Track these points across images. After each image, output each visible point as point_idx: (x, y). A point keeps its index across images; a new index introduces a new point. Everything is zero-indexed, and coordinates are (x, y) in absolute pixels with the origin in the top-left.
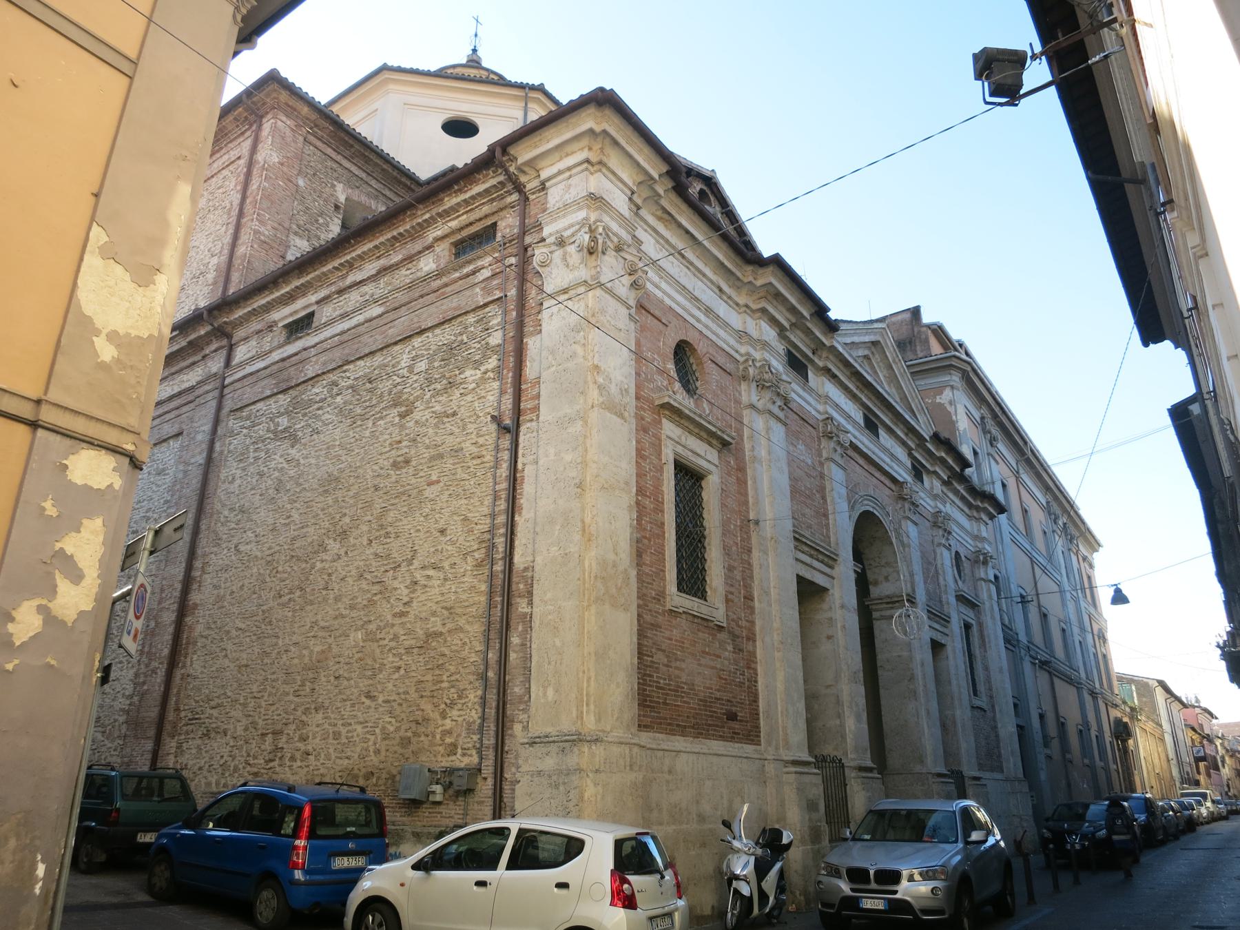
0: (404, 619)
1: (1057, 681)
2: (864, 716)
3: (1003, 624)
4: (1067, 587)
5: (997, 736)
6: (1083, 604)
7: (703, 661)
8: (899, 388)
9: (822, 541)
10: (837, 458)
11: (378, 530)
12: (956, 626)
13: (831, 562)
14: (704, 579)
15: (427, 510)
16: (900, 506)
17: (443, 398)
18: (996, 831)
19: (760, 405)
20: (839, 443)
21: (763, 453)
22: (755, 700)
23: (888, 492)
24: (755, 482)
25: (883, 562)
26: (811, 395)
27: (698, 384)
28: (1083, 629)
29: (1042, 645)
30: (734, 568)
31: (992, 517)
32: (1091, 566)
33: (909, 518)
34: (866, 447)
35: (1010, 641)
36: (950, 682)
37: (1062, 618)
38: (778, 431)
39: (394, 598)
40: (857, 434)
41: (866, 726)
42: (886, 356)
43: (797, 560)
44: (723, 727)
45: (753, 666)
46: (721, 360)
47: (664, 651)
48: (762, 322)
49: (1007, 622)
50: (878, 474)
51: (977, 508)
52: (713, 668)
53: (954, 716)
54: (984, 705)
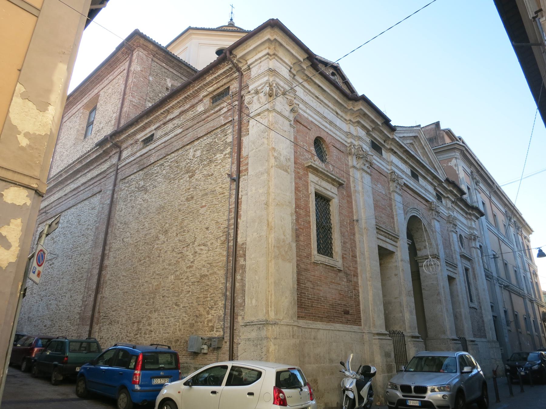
0: (191, 269)
1: (513, 295)
2: (414, 312)
3: (484, 268)
4: (516, 249)
5: (483, 321)
7: (331, 286)
8: (428, 157)
9: (391, 229)
10: (398, 191)
11: (180, 229)
12: (460, 269)
13: (395, 239)
14: (331, 248)
15: (201, 219)
16: (430, 213)
17: (207, 168)
18: (479, 366)
19: (358, 166)
20: (398, 184)
21: (360, 188)
22: (358, 304)
23: (424, 207)
24: (356, 202)
25: (423, 240)
26: (384, 162)
27: (327, 157)
28: (525, 270)
29: (505, 278)
30: (347, 243)
31: (477, 218)
32: (529, 241)
33: (435, 219)
35: (488, 276)
36: (458, 296)
37: (515, 265)
38: (367, 178)
39: (187, 260)
40: (407, 179)
41: (415, 317)
43: (378, 238)
44: (342, 317)
45: (357, 288)
46: (338, 146)
47: (311, 282)
48: (358, 128)
49: (487, 268)
50: (419, 198)
51: (470, 214)
52: (336, 289)
53: (460, 312)
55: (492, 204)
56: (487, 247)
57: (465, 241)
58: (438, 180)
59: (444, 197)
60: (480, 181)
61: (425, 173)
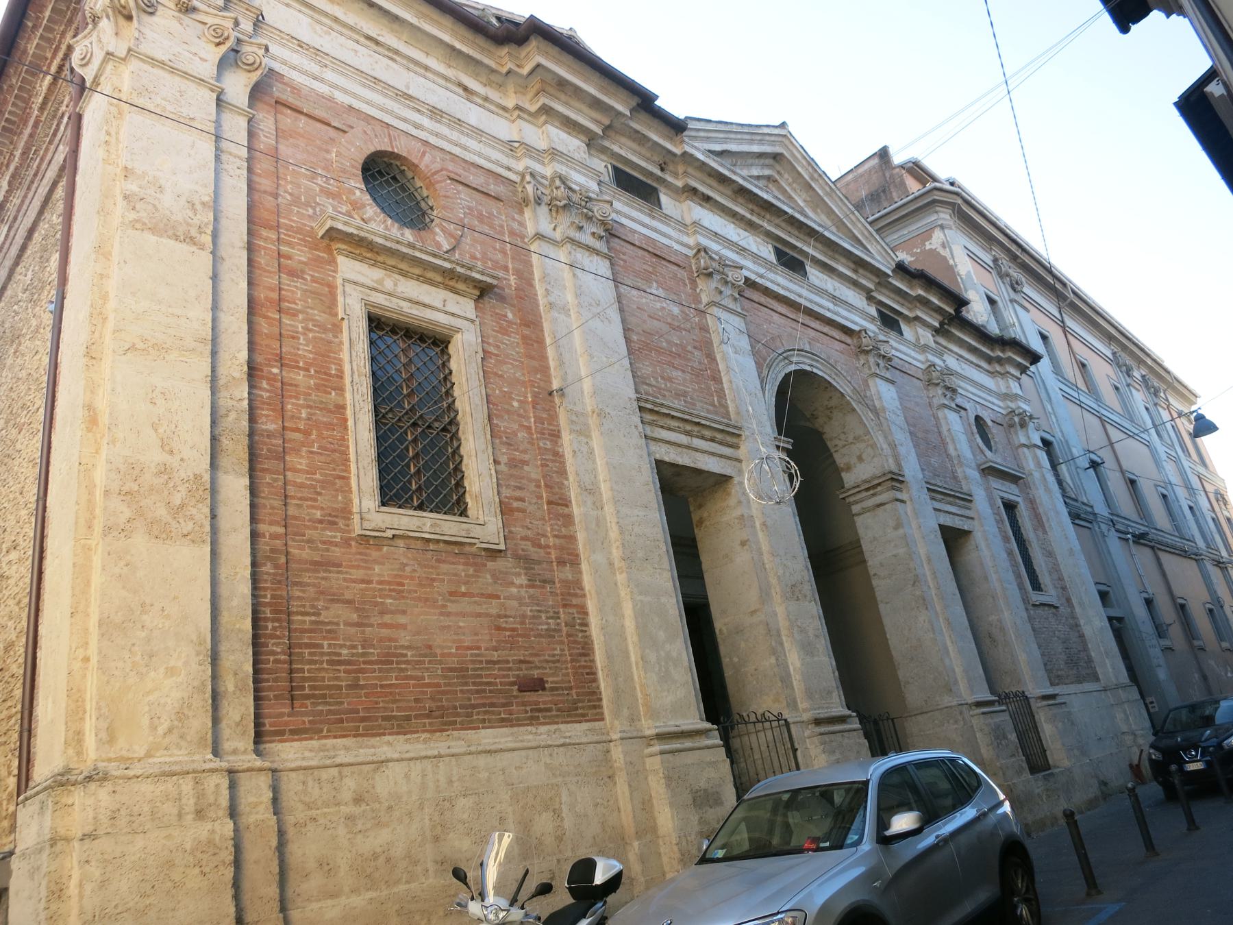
5: (1082, 636)
6: (1186, 464)
7: (452, 607)
8: (830, 212)
16: (862, 362)
22: (586, 650)
26: (669, 225)
29: (1135, 517)
31: (1024, 370)
35: (1080, 516)
36: (986, 578)
42: (799, 174)
47: (349, 602)
51: (999, 361)
52: (479, 615)
53: (1000, 621)
54: (1055, 602)
56: (1067, 441)
58: (871, 272)
59: (908, 320)
61: (826, 255)
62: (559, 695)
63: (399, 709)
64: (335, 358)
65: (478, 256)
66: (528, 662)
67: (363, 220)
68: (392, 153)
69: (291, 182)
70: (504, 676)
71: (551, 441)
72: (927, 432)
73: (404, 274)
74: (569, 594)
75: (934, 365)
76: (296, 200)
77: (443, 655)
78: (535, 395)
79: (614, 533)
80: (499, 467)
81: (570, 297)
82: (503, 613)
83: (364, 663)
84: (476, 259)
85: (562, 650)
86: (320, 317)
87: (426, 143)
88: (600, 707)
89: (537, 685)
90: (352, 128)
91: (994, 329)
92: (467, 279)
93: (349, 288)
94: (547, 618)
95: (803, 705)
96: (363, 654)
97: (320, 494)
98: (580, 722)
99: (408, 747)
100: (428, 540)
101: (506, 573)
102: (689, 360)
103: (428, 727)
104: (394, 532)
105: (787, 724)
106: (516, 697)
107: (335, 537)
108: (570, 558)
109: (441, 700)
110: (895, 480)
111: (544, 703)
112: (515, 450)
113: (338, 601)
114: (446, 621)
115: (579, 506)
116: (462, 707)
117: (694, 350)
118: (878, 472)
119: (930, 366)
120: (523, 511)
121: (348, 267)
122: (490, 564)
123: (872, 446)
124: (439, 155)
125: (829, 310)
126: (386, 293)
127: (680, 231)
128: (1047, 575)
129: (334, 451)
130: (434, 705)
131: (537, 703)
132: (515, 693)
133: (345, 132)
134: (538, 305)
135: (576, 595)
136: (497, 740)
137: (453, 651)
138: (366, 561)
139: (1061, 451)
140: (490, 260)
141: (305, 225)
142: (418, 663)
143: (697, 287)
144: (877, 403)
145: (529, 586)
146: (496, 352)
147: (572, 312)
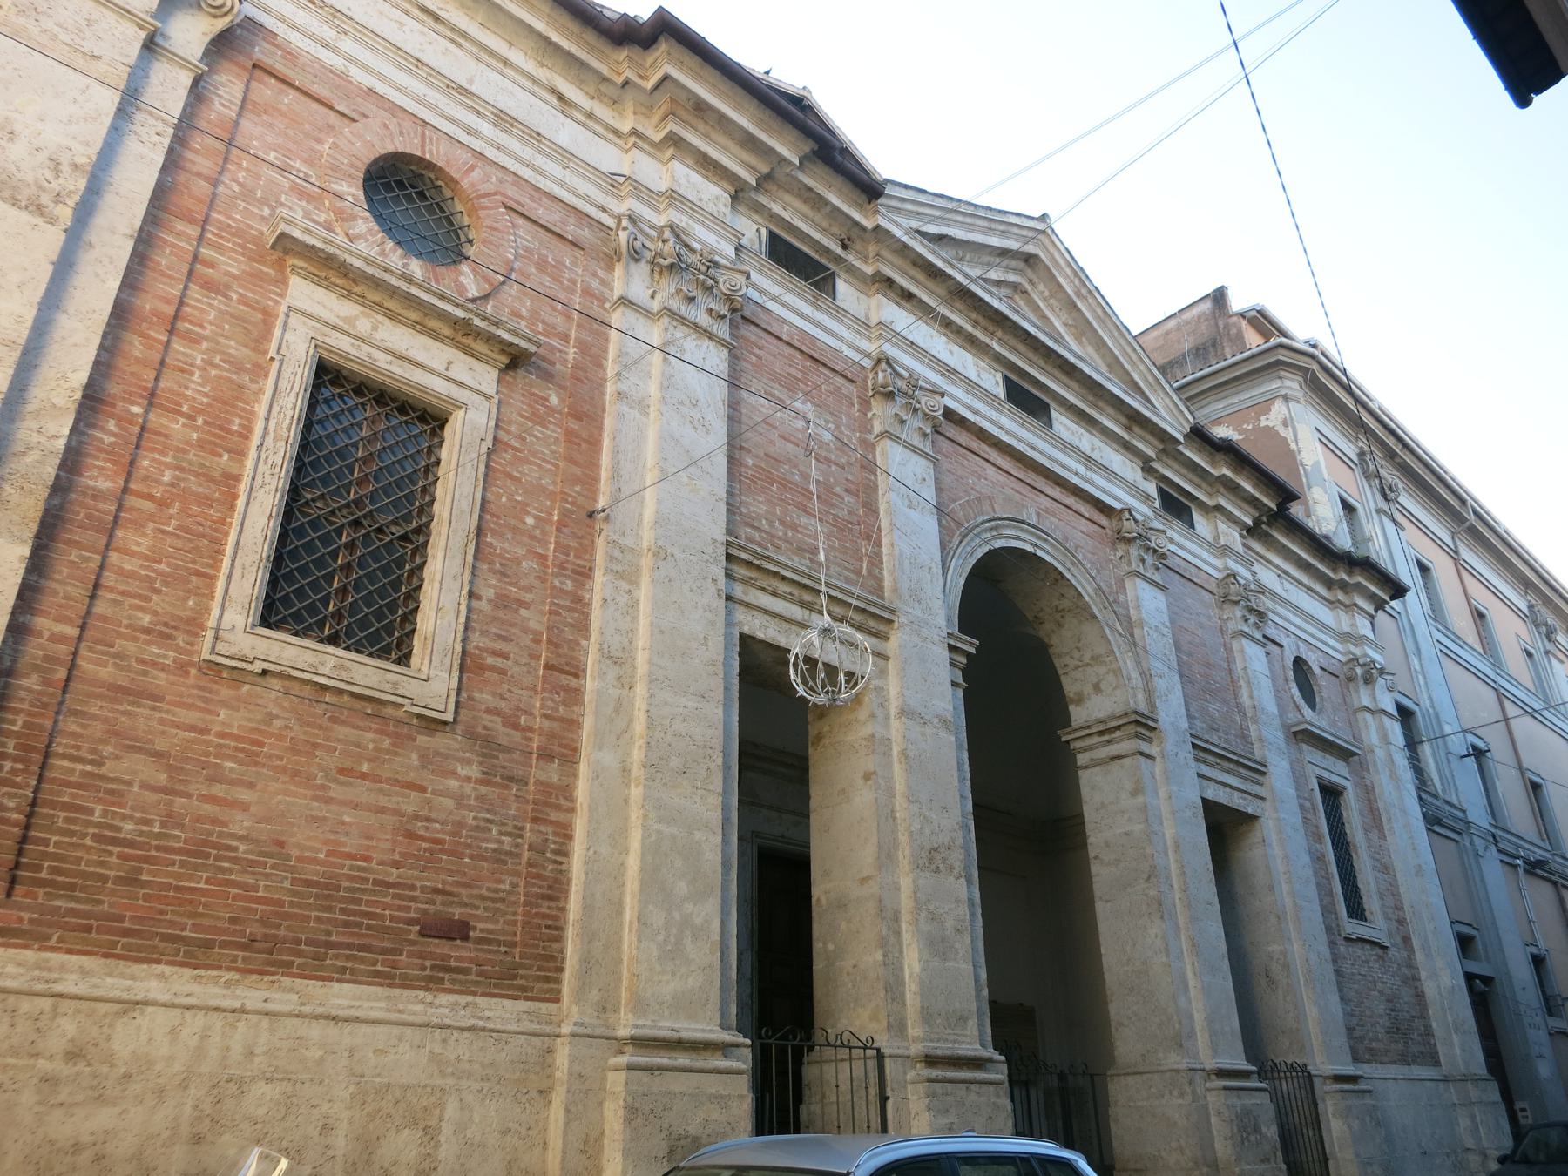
34: (1008, 433)
55: (1463, 572)
57: (1323, 683)
60: (1400, 485)
62: (490, 951)
63: (195, 927)
64: (243, 410)
65: (524, 312)
66: (450, 894)
67: (347, 235)
68: (421, 160)
69: (247, 170)
70: (400, 908)
71: (574, 581)
72: (1208, 665)
73: (393, 317)
74: (547, 804)
75: (1234, 576)
76: (247, 193)
77: (300, 859)
78: (565, 514)
79: (639, 727)
80: (475, 603)
81: (653, 390)
82: (424, 813)
83: (158, 848)
84: (521, 317)
85: (515, 885)
86: (235, 349)
87: (480, 155)
88: (558, 981)
89: (459, 931)
90: (366, 116)
91: (1343, 542)
92: (490, 339)
93: (294, 319)
94: (501, 833)
95: (914, 1030)
96: (159, 836)
97: (158, 592)
98: (516, 998)
99: (196, 988)
100: (324, 688)
101: (447, 756)
102: (833, 505)
103: (239, 964)
104: (266, 666)
105: (880, 1057)
106: (413, 943)
107: (165, 657)
108: (563, 751)
109: (278, 927)
110: (1143, 724)
111: (460, 959)
112: (511, 584)
113: (140, 750)
114: (318, 809)
115: (594, 678)
116: (309, 942)
117: (844, 494)
118: (1119, 710)
119: (1228, 576)
120: (502, 672)
121: (302, 292)
122: (422, 739)
123: (1115, 672)
124: (495, 174)
125: (1076, 474)
126: (354, 337)
127: (858, 332)
128: (1375, 896)
129: (202, 536)
130: (261, 932)
131: (448, 957)
132: (412, 937)
133: (354, 121)
134: (604, 394)
135: (558, 808)
136: (357, 1003)
137: (322, 856)
138: (207, 700)
139: (1426, 727)
140: (543, 322)
141: (252, 227)
142: (252, 863)
143: (870, 409)
144: (1132, 612)
145: (478, 781)
146: (517, 445)
147: (652, 409)
